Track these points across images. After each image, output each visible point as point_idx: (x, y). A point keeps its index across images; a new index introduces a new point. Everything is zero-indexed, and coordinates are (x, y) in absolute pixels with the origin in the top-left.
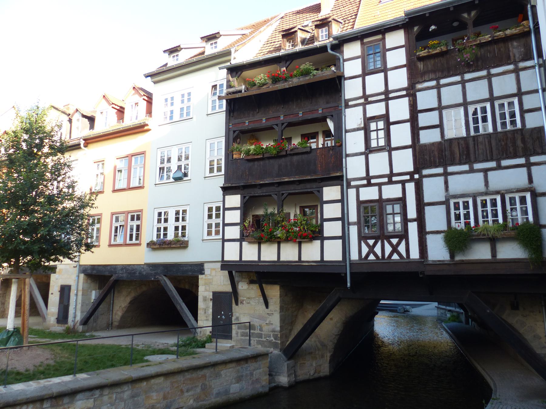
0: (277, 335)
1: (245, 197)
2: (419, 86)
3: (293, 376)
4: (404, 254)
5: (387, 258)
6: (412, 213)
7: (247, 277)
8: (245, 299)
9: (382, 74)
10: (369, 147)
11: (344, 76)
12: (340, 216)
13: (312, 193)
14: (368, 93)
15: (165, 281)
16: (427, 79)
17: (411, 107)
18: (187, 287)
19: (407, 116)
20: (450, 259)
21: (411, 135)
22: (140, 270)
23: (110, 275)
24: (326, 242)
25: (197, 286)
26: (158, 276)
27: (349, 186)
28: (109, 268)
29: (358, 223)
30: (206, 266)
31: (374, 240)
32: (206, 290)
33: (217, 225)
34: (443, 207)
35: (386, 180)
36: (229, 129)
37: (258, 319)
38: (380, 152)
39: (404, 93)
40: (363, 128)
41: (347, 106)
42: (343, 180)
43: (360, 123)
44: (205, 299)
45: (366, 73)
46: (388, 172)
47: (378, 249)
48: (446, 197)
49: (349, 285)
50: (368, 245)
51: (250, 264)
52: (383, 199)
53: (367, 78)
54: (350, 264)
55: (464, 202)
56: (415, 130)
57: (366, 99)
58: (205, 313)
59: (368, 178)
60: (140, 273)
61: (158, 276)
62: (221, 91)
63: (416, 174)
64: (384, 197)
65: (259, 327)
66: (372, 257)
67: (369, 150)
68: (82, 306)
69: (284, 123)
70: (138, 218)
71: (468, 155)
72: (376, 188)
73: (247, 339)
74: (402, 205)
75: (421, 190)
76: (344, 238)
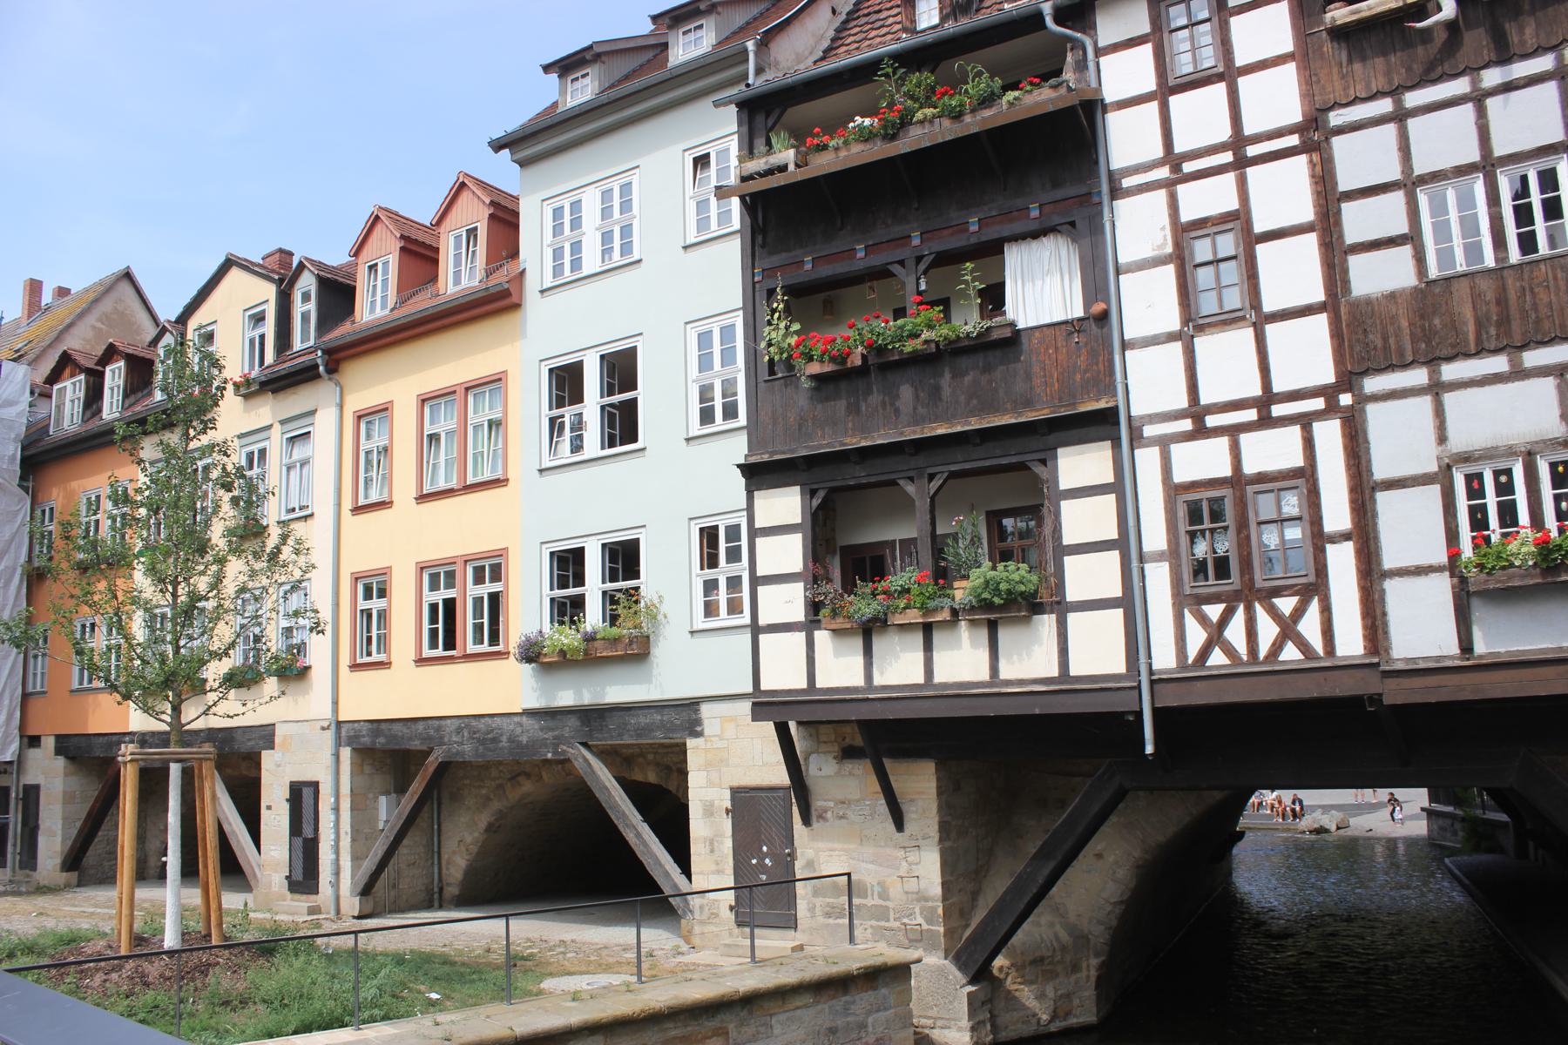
0: (934, 909)
1: (813, 493)
2: (1336, 118)
3: (988, 1026)
4: (1317, 644)
5: (1266, 657)
6: (1337, 514)
7: (833, 738)
8: (831, 804)
9: (1221, 88)
10: (1193, 316)
11: (1102, 100)
12: (1115, 536)
13: (1022, 467)
14: (1179, 148)
15: (586, 760)
16: (1364, 95)
17: (1316, 183)
18: (652, 777)
19: (1307, 213)
20: (1458, 651)
21: (1323, 272)
23: (424, 748)
24: (1072, 618)
25: (683, 773)
26: (565, 748)
27: (1136, 438)
28: (420, 726)
29: (1172, 555)
30: (706, 710)
31: (1223, 606)
32: (710, 784)
33: (734, 583)
34: (1435, 490)
35: (1251, 415)
36: (754, 284)
37: (871, 862)
38: (1227, 327)
39: (1293, 140)
40: (1170, 255)
41: (1116, 192)
42: (1117, 423)
43: (1159, 243)
44: (709, 811)
45: (1168, 87)
46: (1256, 390)
47: (1235, 633)
48: (1439, 458)
49: (1149, 749)
50: (1203, 620)
51: (840, 698)
52: (1246, 476)
53: (1175, 101)
54: (1152, 683)
55: (1497, 474)
56: (1335, 255)
57: (1176, 168)
58: (712, 851)
59: (1197, 411)
60: (510, 740)
61: (565, 748)
62: (723, 171)
63: (1345, 391)
64: (1249, 468)
65: (877, 889)
66: (1217, 658)
67: (1193, 324)
68: (353, 840)
69: (922, 257)
70: (497, 573)
71: (1504, 322)
72: (1223, 442)
73: (843, 925)
74: (1305, 491)
75: (1361, 440)
76: (1130, 603)
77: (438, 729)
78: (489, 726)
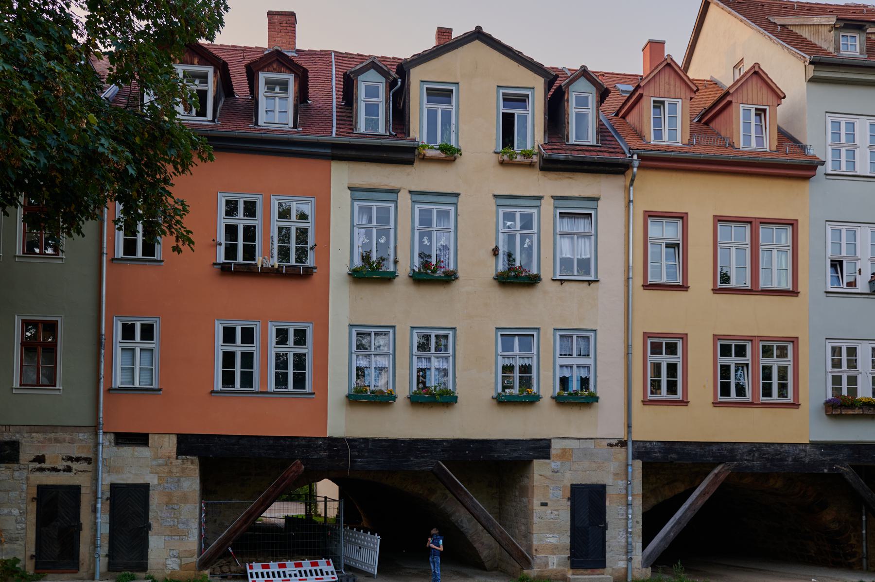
22: (798, 454)
60: (794, 460)
61: (839, 467)
78: (777, 450)
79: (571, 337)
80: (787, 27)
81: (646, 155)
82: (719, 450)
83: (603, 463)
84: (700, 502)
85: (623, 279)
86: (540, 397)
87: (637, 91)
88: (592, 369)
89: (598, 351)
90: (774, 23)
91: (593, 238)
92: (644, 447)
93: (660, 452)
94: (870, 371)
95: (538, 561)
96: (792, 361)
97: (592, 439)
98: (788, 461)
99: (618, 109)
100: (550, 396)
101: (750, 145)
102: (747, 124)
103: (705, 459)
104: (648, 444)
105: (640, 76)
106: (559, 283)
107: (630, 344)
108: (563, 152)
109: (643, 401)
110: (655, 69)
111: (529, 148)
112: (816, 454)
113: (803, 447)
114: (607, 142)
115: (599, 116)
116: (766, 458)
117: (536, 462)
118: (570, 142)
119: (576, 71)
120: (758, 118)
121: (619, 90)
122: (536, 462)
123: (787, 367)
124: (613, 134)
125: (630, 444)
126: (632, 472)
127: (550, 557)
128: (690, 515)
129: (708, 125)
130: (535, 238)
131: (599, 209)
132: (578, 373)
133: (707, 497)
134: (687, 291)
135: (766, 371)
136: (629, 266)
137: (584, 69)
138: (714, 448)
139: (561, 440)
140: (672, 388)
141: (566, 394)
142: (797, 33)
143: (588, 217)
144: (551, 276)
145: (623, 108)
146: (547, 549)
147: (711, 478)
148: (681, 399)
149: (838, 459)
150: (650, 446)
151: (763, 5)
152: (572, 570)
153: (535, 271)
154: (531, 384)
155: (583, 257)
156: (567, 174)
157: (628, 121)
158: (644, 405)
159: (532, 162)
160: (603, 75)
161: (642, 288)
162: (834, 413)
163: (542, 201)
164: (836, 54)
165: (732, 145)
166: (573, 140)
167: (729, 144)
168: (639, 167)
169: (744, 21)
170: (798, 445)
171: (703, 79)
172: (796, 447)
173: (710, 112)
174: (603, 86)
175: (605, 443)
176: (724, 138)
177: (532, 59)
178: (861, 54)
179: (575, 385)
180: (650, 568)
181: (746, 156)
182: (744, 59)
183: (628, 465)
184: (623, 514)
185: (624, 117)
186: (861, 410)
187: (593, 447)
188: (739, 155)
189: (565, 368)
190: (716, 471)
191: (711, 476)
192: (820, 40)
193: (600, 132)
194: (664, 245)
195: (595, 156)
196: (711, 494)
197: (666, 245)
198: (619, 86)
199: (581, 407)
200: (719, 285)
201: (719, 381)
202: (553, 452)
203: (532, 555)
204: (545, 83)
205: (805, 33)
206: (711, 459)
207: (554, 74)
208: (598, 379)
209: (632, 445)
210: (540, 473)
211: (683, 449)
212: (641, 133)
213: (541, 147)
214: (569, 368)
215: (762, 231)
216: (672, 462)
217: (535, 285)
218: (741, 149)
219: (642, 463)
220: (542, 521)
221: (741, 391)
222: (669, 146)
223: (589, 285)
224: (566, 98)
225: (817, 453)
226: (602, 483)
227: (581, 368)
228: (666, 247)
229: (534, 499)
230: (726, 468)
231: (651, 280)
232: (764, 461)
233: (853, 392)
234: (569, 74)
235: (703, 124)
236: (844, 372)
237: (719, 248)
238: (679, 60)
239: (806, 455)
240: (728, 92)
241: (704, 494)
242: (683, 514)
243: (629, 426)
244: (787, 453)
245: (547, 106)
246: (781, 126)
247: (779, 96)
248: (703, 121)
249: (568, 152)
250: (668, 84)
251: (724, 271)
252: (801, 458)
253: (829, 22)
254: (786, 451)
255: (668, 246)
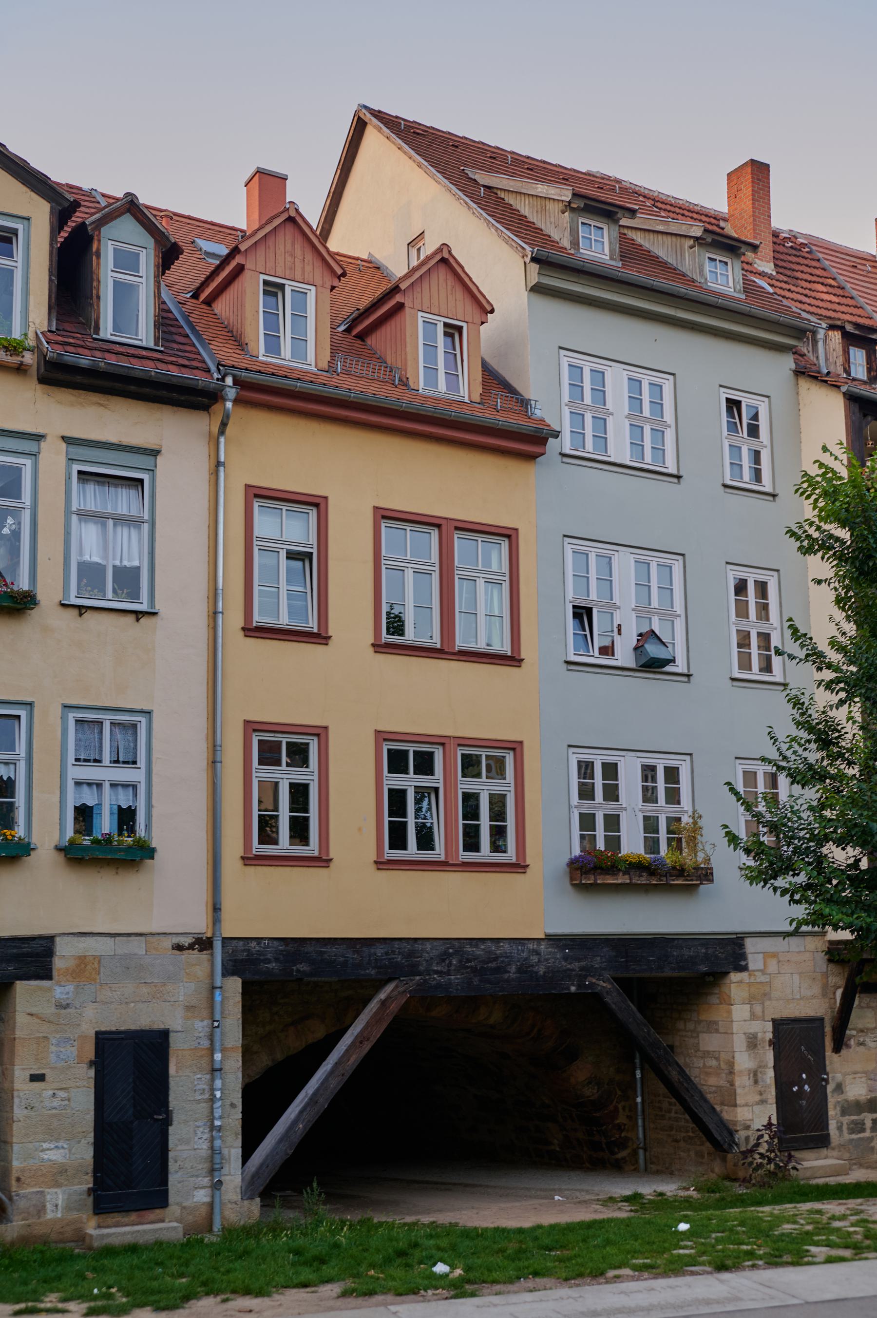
22: (526, 959)
60: (519, 970)
61: (594, 981)
77: (411, 954)
78: (490, 952)
79: (100, 723)
80: (495, 191)
81: (249, 380)
82: (387, 953)
83: (164, 985)
84: (353, 1059)
85: (205, 614)
86: (32, 846)
87: (234, 258)
88: (142, 789)
89: (155, 755)
90: (475, 180)
91: (146, 527)
92: (244, 951)
93: (277, 960)
94: (641, 807)
95: (22, 1204)
96: (512, 785)
97: (141, 935)
98: (509, 972)
99: (198, 285)
100: (53, 845)
101: (437, 387)
102: (431, 347)
103: (363, 972)
104: (253, 944)
105: (242, 231)
106: (75, 612)
107: (218, 743)
108: (87, 352)
109: (243, 858)
110: (267, 223)
111: (16, 334)
112: (556, 959)
113: (535, 946)
114: (175, 346)
115: (159, 293)
116: (471, 967)
117: (20, 987)
118: (102, 335)
119: (117, 200)
120: (449, 340)
121: (201, 249)
122: (20, 987)
123: (505, 795)
124: (188, 331)
125: (218, 945)
126: (222, 1002)
127: (49, 1193)
128: (335, 1084)
129: (363, 341)
130: (26, 516)
131: (159, 471)
132: (113, 797)
133: (367, 1047)
134: (327, 644)
135: (472, 802)
136: (216, 589)
137: (132, 201)
138: (379, 951)
139: (76, 939)
140: (299, 831)
141: (86, 841)
142: (511, 205)
143: (137, 486)
144: (59, 597)
145: (208, 286)
146: (42, 1176)
147: (374, 1011)
148: (316, 854)
149: (592, 966)
150: (257, 948)
151: (457, 147)
152: (96, 1217)
153: (23, 584)
154: (13, 818)
155: (126, 563)
156: (95, 397)
157: (216, 311)
158: (245, 865)
159: (22, 364)
160: (172, 216)
161: (242, 633)
162: (583, 882)
163: (43, 444)
164: (572, 252)
165: (404, 383)
166: (107, 331)
167: (400, 380)
168: (237, 401)
169: (422, 166)
170: (527, 942)
171: (356, 255)
172: (523, 945)
173: (367, 317)
174: (168, 238)
175: (168, 943)
176: (391, 368)
177: (26, 162)
178: (611, 258)
179: (106, 824)
180: (258, 1200)
181: (429, 405)
182: (426, 233)
183: (214, 988)
184: (204, 1090)
185: (209, 302)
186: (627, 876)
187: (144, 953)
188: (417, 402)
189: (85, 787)
190: (382, 995)
191: (373, 1006)
192: (548, 223)
193: (163, 325)
194: (283, 555)
195: (151, 369)
196: (373, 1040)
197: (287, 553)
198: (201, 243)
199: (118, 868)
200: (385, 637)
201: (387, 819)
202: (58, 964)
203: (10, 1192)
204: (51, 213)
205: (524, 207)
206: (373, 972)
207: (72, 200)
208: (155, 812)
209: (223, 947)
210: (28, 1011)
211: (322, 953)
212: (241, 337)
213: (41, 336)
214: (95, 787)
215: (460, 544)
216: (301, 980)
217: (24, 613)
218: (421, 391)
219: (243, 983)
220: (33, 1113)
221: (425, 840)
222: (292, 369)
223: (138, 620)
224: (94, 249)
225: (558, 956)
226: (162, 1027)
227: (120, 789)
228: (288, 558)
229: (16, 1067)
230: (401, 989)
231: (258, 619)
232: (467, 973)
233: (614, 842)
234: (103, 203)
235: (354, 336)
236: (600, 807)
237: (383, 567)
238: (313, 215)
239: (539, 961)
240: (398, 286)
241: (361, 1042)
242: (322, 1084)
243: (216, 909)
244: (507, 957)
245: (55, 258)
246: (487, 359)
247: (485, 309)
248: (355, 331)
249: (98, 354)
250: (292, 255)
251: (396, 611)
252: (532, 966)
253: (561, 196)
254: (506, 953)
255: (291, 556)
